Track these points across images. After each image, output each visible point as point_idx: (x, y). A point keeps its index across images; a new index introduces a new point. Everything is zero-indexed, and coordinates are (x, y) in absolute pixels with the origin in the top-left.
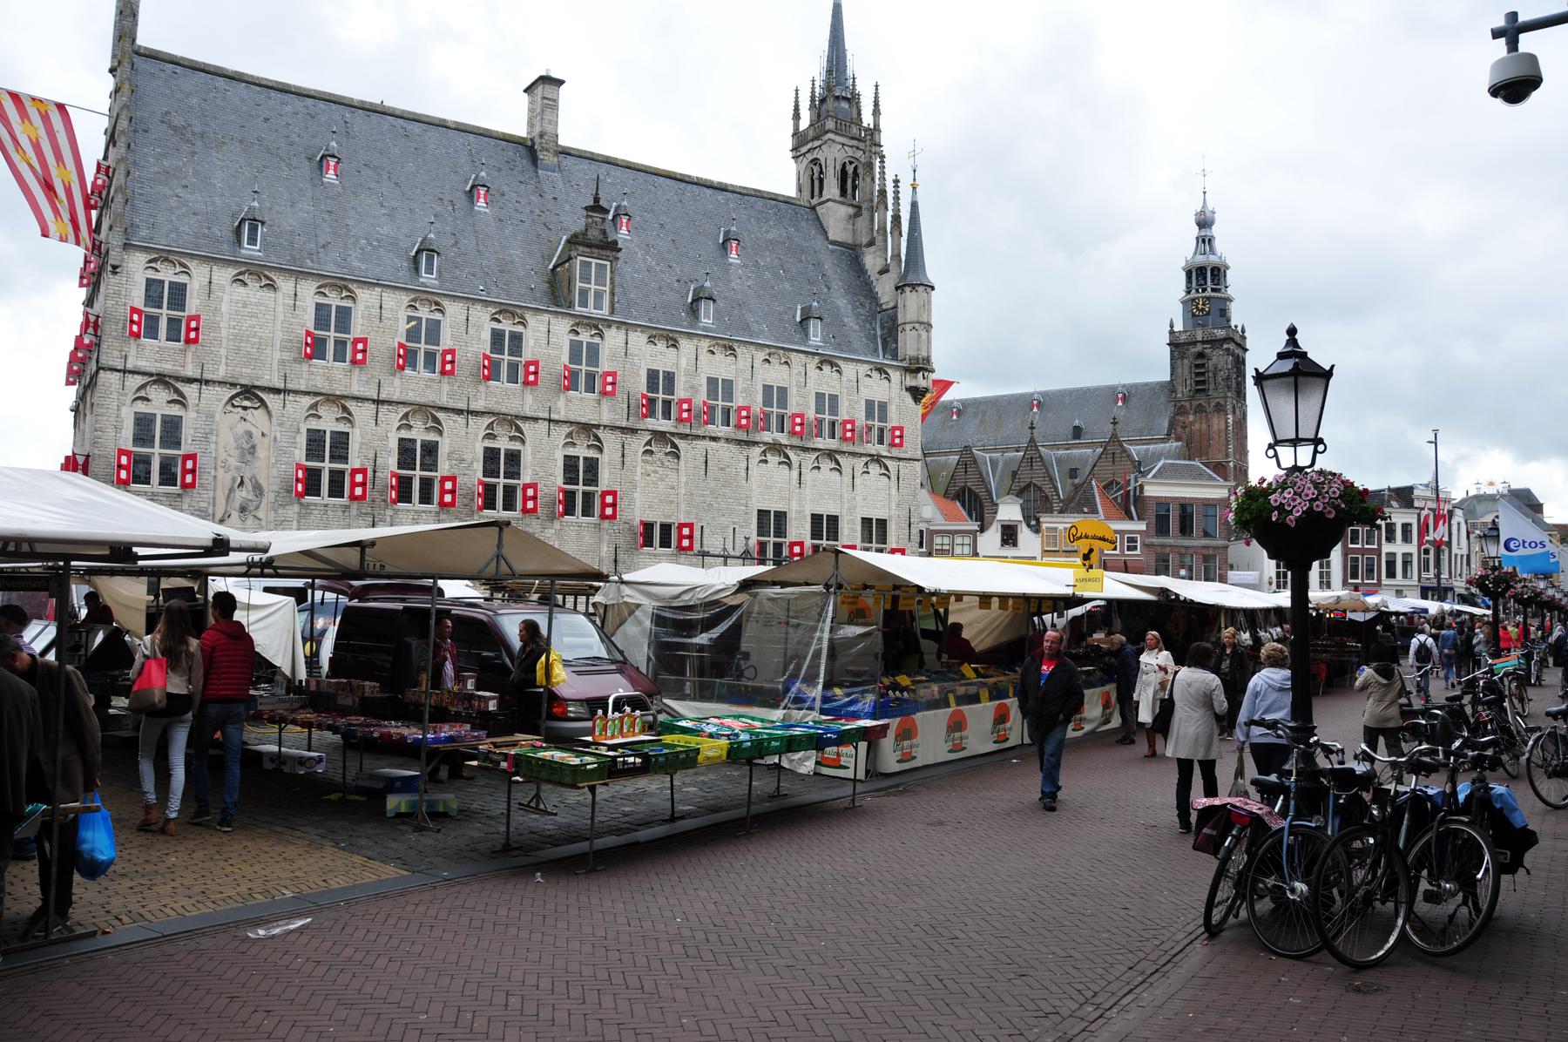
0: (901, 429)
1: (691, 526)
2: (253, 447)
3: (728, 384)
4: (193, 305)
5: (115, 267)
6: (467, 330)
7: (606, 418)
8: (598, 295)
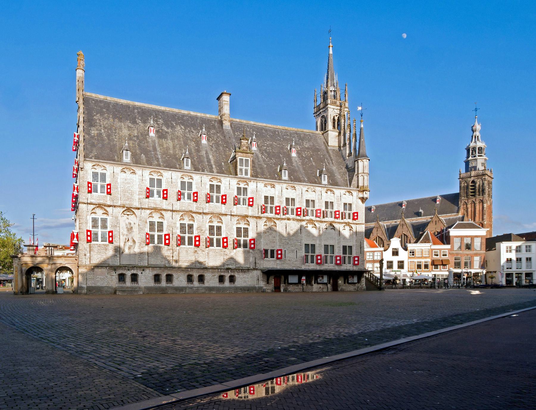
0: (357, 213)
1: (281, 250)
2: (132, 228)
3: (293, 200)
5: (82, 168)
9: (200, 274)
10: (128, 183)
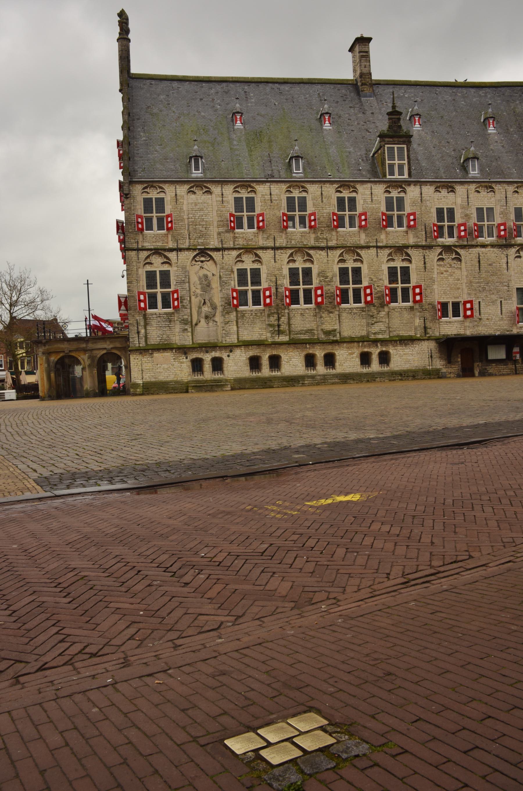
1: (471, 302)
3: (490, 210)
4: (168, 209)
6: (321, 200)
7: (412, 240)
8: (401, 167)
9: (327, 351)
10: (201, 210)
